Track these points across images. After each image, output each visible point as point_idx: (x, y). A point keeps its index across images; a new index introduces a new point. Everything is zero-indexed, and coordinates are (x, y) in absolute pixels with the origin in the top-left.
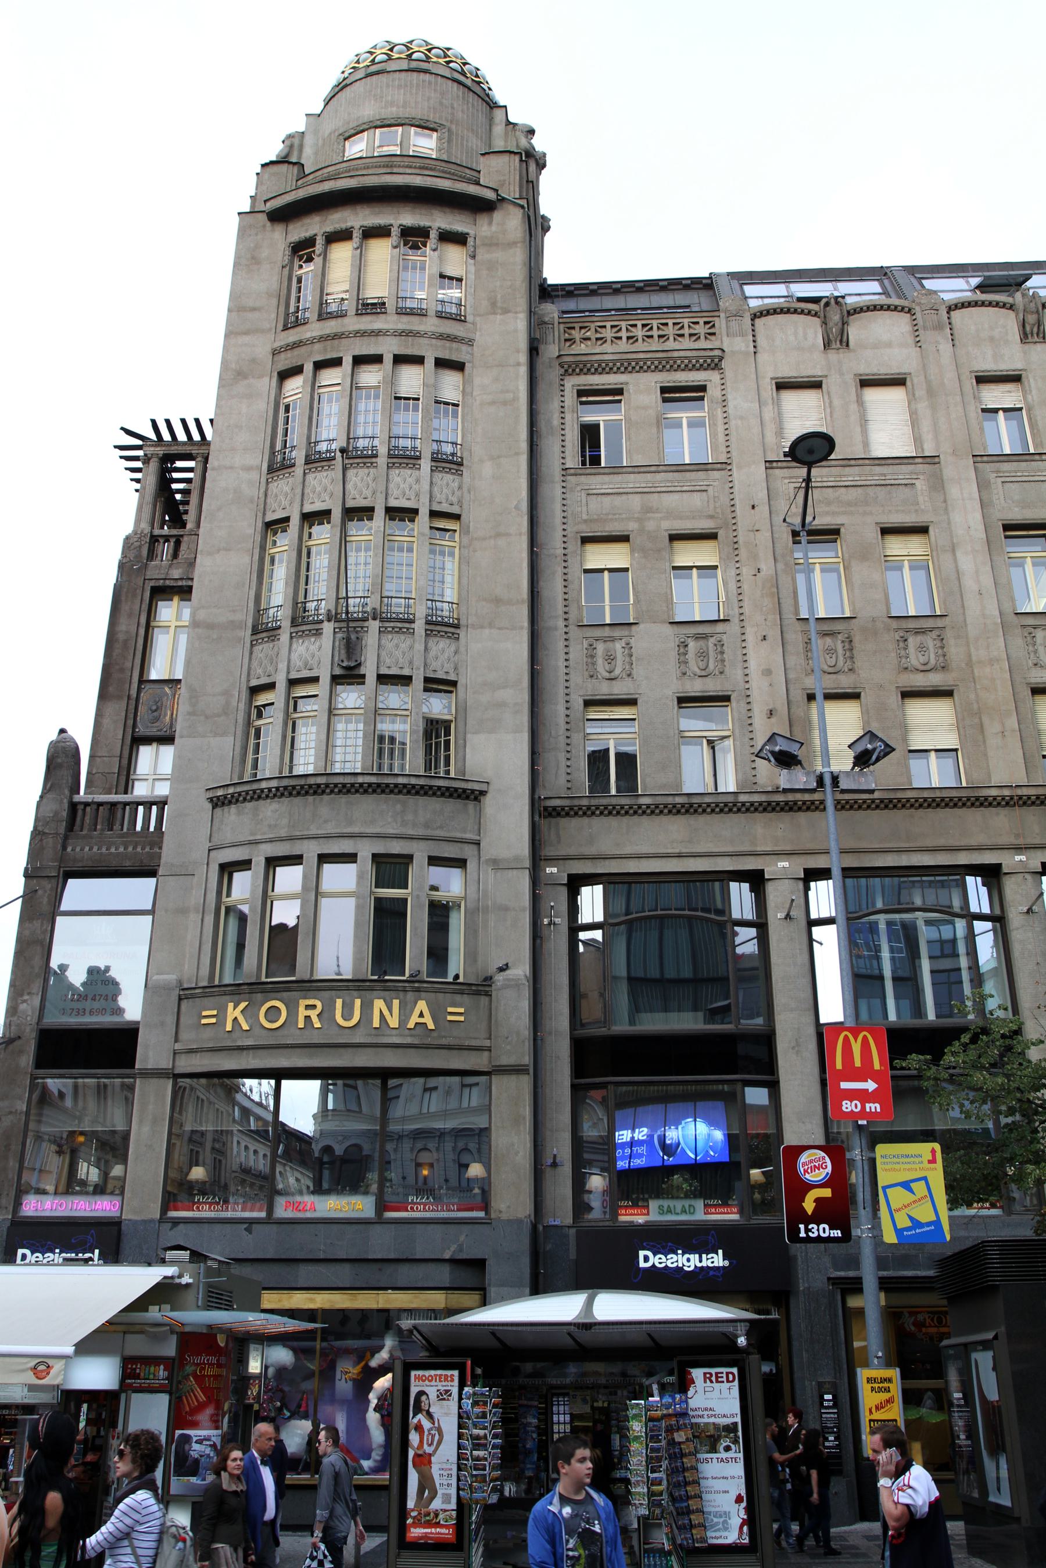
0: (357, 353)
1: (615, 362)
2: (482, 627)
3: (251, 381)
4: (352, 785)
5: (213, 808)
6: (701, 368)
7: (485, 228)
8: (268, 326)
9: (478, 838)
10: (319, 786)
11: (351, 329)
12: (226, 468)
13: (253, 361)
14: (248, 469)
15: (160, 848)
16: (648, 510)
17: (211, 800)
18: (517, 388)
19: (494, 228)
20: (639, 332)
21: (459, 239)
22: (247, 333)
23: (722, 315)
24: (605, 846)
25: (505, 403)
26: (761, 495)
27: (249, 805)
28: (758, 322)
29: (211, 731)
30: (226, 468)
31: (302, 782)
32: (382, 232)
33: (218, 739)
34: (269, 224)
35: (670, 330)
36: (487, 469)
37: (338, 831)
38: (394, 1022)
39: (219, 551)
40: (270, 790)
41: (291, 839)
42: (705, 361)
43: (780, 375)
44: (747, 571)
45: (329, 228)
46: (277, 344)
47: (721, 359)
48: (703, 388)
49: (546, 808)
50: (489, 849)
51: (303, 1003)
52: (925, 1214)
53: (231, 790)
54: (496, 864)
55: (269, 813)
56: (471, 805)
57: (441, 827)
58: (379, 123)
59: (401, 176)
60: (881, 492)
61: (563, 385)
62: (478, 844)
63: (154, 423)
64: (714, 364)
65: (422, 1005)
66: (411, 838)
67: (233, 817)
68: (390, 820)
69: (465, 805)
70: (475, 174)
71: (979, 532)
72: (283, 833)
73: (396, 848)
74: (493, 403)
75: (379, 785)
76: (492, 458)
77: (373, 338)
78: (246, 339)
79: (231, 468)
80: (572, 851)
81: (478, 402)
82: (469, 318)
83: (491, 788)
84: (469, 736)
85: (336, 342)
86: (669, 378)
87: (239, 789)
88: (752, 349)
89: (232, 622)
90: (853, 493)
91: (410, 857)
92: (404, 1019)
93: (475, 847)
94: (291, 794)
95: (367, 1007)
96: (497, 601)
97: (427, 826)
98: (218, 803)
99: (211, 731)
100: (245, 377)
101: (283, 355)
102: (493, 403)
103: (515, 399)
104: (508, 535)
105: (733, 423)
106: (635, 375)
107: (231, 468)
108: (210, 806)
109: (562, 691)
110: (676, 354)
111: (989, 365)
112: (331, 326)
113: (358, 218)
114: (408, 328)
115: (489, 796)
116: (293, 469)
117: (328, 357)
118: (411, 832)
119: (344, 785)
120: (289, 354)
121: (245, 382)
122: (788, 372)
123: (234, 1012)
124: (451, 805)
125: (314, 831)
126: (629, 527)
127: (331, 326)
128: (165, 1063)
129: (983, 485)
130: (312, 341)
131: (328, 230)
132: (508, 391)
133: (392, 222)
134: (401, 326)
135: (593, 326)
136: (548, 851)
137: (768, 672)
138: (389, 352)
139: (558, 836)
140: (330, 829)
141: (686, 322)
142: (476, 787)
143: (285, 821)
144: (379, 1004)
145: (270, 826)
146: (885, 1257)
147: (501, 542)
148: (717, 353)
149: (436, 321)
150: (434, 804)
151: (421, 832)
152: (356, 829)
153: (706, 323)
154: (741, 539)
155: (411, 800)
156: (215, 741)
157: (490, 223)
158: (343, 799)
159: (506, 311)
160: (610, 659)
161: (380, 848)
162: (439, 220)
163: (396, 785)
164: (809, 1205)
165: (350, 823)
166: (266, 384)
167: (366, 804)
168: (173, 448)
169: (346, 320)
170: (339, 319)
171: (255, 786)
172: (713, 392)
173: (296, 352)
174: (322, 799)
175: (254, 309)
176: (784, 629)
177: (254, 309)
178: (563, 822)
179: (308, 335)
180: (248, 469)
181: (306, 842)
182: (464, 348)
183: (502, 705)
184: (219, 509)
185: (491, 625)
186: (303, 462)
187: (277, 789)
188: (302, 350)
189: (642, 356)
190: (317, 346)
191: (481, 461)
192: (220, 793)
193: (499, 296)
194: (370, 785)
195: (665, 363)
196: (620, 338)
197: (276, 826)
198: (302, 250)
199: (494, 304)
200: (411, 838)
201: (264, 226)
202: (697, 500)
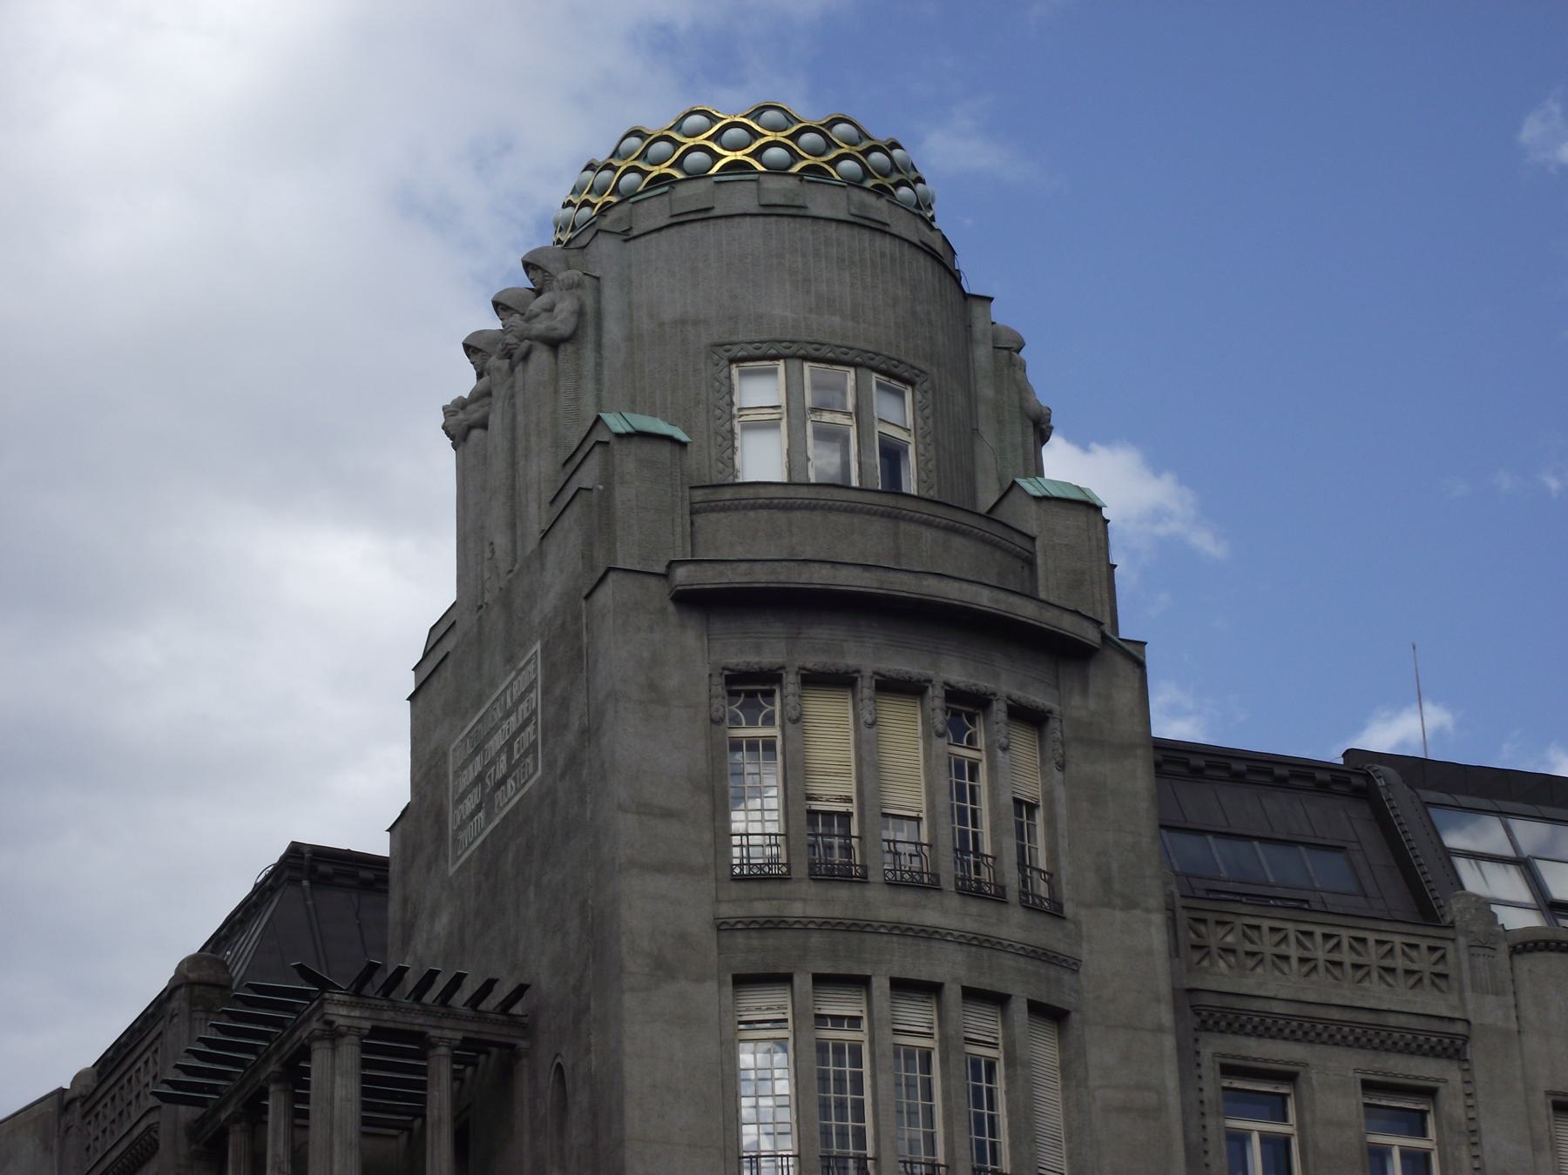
0: (897, 975)
1: (1289, 1018)
6: (1433, 1053)
7: (1076, 700)
19: (1092, 704)
20: (1320, 953)
21: (1029, 718)
22: (662, 868)
23: (1462, 941)
28: (1525, 963)
32: (911, 689)
34: (671, 608)
35: (1372, 955)
42: (1440, 1041)
43: (1559, 1088)
45: (813, 662)
47: (1466, 1039)
48: (1430, 1093)
58: (810, 350)
59: (956, 585)
61: (1198, 1053)
70: (1027, 545)
82: (1069, 909)
86: (1377, 1066)
88: (1514, 1026)
101: (740, 939)
106: (1319, 1047)
110: (1392, 1020)
112: (840, 901)
113: (867, 653)
120: (755, 940)
127: (840, 901)
130: (804, 926)
131: (810, 665)
133: (931, 673)
134: (971, 925)
135: (1239, 922)
141: (1398, 940)
148: (1459, 1028)
149: (1016, 915)
153: (1432, 949)
157: (1085, 692)
159: (1130, 904)
162: (1009, 681)
170: (856, 889)
172: (1452, 1104)
173: (771, 939)
175: (668, 814)
177: (668, 814)
179: (797, 910)
182: (1067, 977)
189: (1335, 1014)
190: (816, 940)
193: (1115, 867)
195: (1368, 1033)
196: (1286, 958)
198: (748, 686)
201: (663, 610)
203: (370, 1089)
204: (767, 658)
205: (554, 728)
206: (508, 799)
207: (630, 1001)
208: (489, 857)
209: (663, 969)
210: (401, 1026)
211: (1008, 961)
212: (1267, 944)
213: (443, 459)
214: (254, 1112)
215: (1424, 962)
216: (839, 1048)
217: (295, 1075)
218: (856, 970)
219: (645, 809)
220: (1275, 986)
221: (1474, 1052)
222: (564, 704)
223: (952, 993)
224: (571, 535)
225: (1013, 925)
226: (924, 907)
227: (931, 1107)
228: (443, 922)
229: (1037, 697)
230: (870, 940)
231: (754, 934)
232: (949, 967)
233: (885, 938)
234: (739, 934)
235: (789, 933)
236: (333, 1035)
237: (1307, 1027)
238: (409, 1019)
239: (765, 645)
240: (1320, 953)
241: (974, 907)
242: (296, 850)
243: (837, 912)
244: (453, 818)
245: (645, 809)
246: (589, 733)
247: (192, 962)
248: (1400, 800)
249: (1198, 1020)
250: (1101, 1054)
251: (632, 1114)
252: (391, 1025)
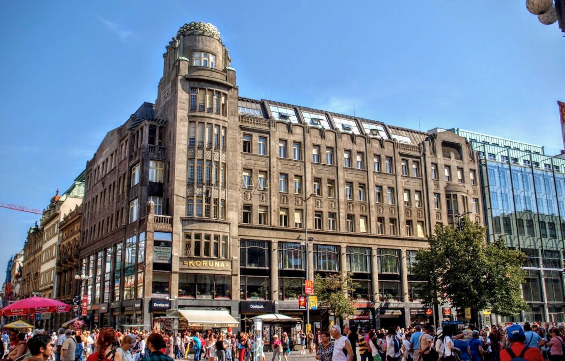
14: (185, 145)
16: (255, 164)
22: (182, 109)
24: (247, 234)
26: (275, 165)
38: (218, 266)
44: (272, 181)
48: (266, 138)
51: (204, 261)
52: (314, 306)
54: (233, 238)
60: (295, 167)
64: (268, 133)
65: (222, 263)
71: (310, 179)
73: (218, 233)
90: (290, 167)
92: (220, 265)
95: (214, 263)
96: (233, 184)
105: (271, 147)
111: (315, 143)
122: (281, 137)
123: (191, 262)
124: (225, 225)
125: (203, 229)
126: (253, 168)
128: (178, 270)
129: (312, 169)
134: (216, 117)
137: (274, 202)
140: (206, 229)
144: (216, 263)
146: (310, 310)
150: (223, 225)
154: (272, 173)
156: (181, 207)
158: (209, 223)
159: (234, 116)
160: (247, 196)
164: (302, 304)
165: (210, 228)
177: (183, 103)
180: (185, 145)
183: (233, 206)
199: (232, 113)
202: (264, 163)
203: (150, 130)
204: (196, 86)
205: (172, 92)
206: (167, 99)
207: (178, 124)
208: (165, 106)
209: (181, 120)
212: (250, 121)
213: (163, 60)
214: (138, 132)
215: (267, 124)
217: (142, 129)
219: (181, 102)
220: (250, 126)
221: (271, 133)
222: (173, 89)
223: (214, 125)
224: (175, 70)
225: (221, 117)
228: (160, 112)
229: (226, 92)
232: (214, 122)
236: (146, 125)
237: (253, 130)
239: (196, 84)
240: (255, 122)
242: (145, 103)
244: (162, 100)
245: (181, 102)
246: (175, 93)
247: (133, 115)
248: (267, 105)
250: (229, 132)
251: (177, 136)
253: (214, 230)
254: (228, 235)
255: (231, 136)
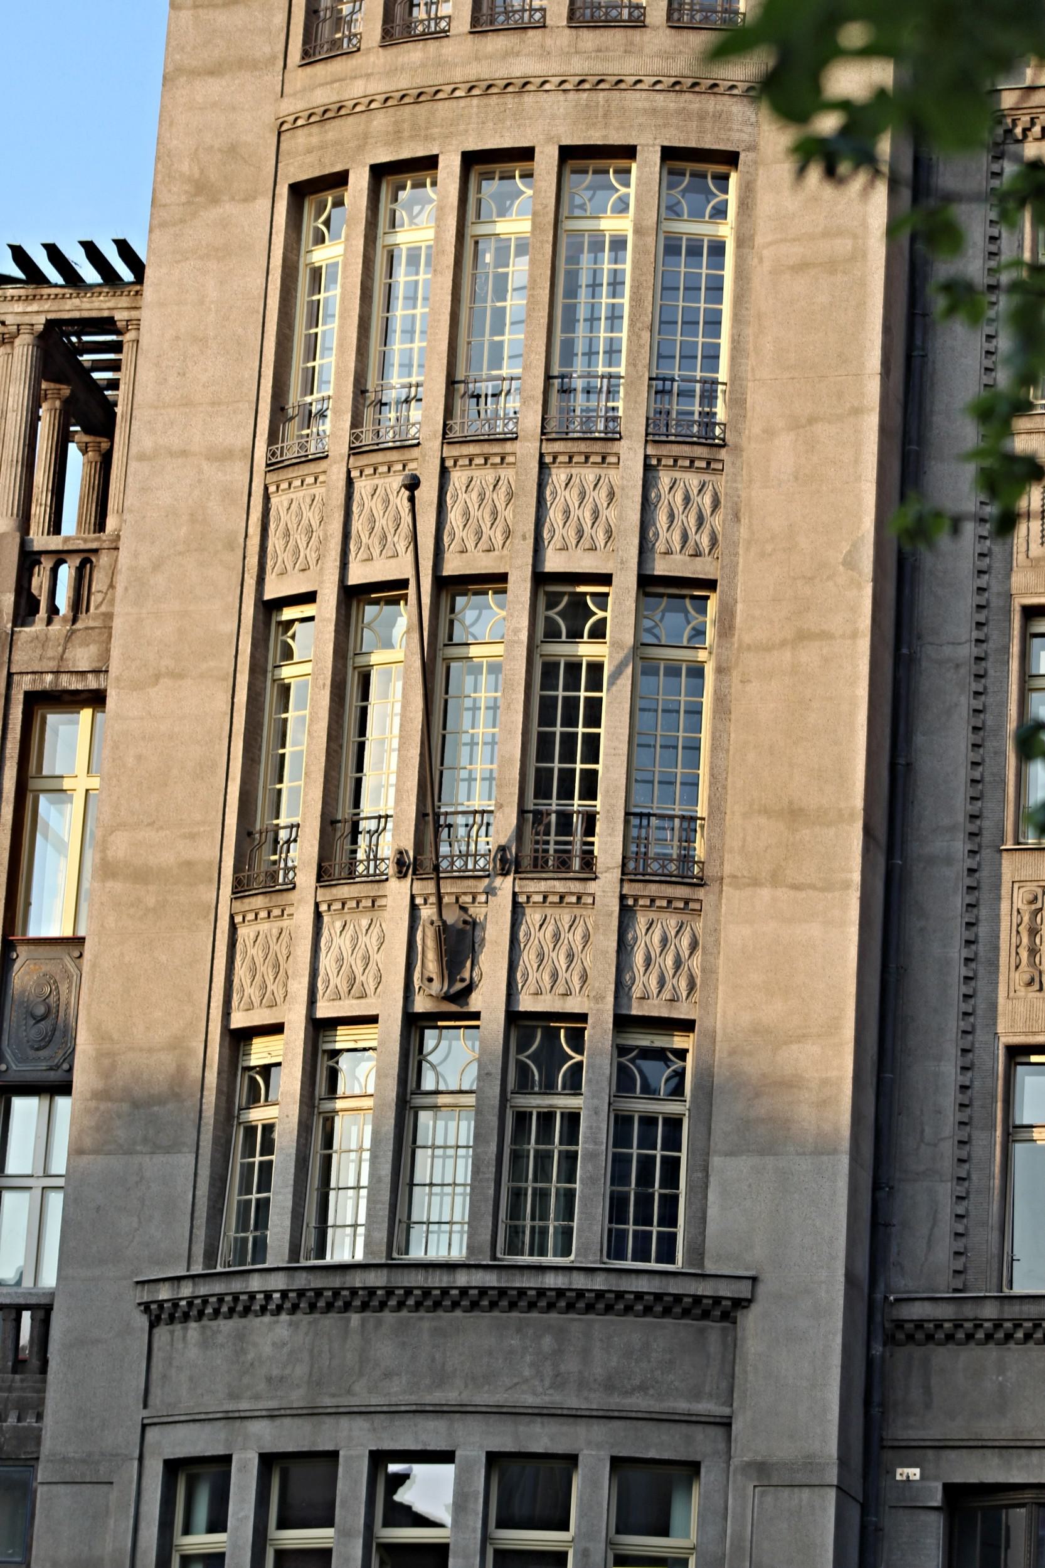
2: (755, 883)
3: (228, 208)
4: (445, 1291)
5: (152, 1326)
8: (267, 49)
9: (726, 1411)
10: (371, 1291)
11: (458, 75)
12: (171, 454)
13: (232, 150)
14: (223, 456)
15: (40, 1417)
17: (146, 1307)
18: (864, 224)
22: (215, 71)
25: (832, 266)
27: (225, 1326)
29: (145, 1140)
30: (171, 454)
31: (336, 1281)
33: (160, 1159)
36: (783, 454)
37: (413, 1399)
39: (157, 677)
40: (268, 1296)
41: (313, 1413)
46: (289, 106)
49: (899, 1324)
50: (749, 1442)
53: (186, 1290)
55: (267, 1350)
56: (714, 1330)
57: (643, 1388)
62: (726, 1424)
63: (19, 255)
66: (575, 1416)
67: (193, 1352)
68: (527, 1373)
69: (702, 1331)
72: (297, 1398)
73: (541, 1439)
74: (802, 267)
75: (502, 1292)
76: (795, 425)
77: (510, 101)
78: (212, 88)
79: (184, 453)
80: (955, 1430)
81: (767, 265)
83: (762, 1289)
84: (716, 1161)
85: (422, 110)
87: (203, 1289)
89: (189, 864)
91: (572, 1460)
93: (719, 1432)
94: (312, 1307)
96: (794, 814)
97: (609, 1386)
98: (158, 1315)
99: (145, 1140)
100: (215, 201)
102: (802, 267)
103: (859, 255)
104: (825, 636)
107: (184, 453)
108: (143, 1321)
109: (953, 1025)
114: (599, 67)
115: (755, 1310)
116: (323, 465)
117: (405, 154)
118: (572, 1401)
119: (427, 1292)
121: (213, 213)
125: (362, 1397)
130: (367, 106)
132: (840, 233)
134: (578, 66)
136: (902, 1430)
138: (549, 140)
139: (927, 1390)
140: (397, 1392)
142: (725, 1290)
143: (301, 1370)
145: (269, 1380)
147: (810, 656)
150: (630, 1331)
151: (596, 1401)
152: (450, 1396)
155: (575, 1323)
158: (426, 1321)
161: (504, 1443)
163: (541, 1292)
165: (441, 1379)
166: (263, 218)
167: (477, 1333)
168: (69, 304)
169: (447, 48)
170: (432, 46)
171: (236, 1286)
173: (335, 130)
174: (379, 1323)
176: (816, 1489)
178: (941, 1356)
179: (357, 89)
180: (223, 456)
181: (344, 1421)
184: (157, 567)
185: (775, 879)
186: (345, 450)
187: (284, 1294)
188: (347, 127)
190: (380, 121)
191: (769, 433)
192: (164, 1293)
194: (483, 1291)
197: (282, 1379)
200: (575, 1416)
210: (86, 314)
211: (636, 100)
216: (694, 251)
218: (420, 153)
226: (518, 54)
227: (575, 306)
230: (443, 109)
231: (315, 129)
233: (462, 103)
234: (300, 132)
235: (351, 119)
238: (96, 305)
241: (589, 39)
243: (403, 82)
249: (1000, 131)
252: (76, 315)
253: (484, 1398)
254: (701, 1444)
255: (795, 252)
